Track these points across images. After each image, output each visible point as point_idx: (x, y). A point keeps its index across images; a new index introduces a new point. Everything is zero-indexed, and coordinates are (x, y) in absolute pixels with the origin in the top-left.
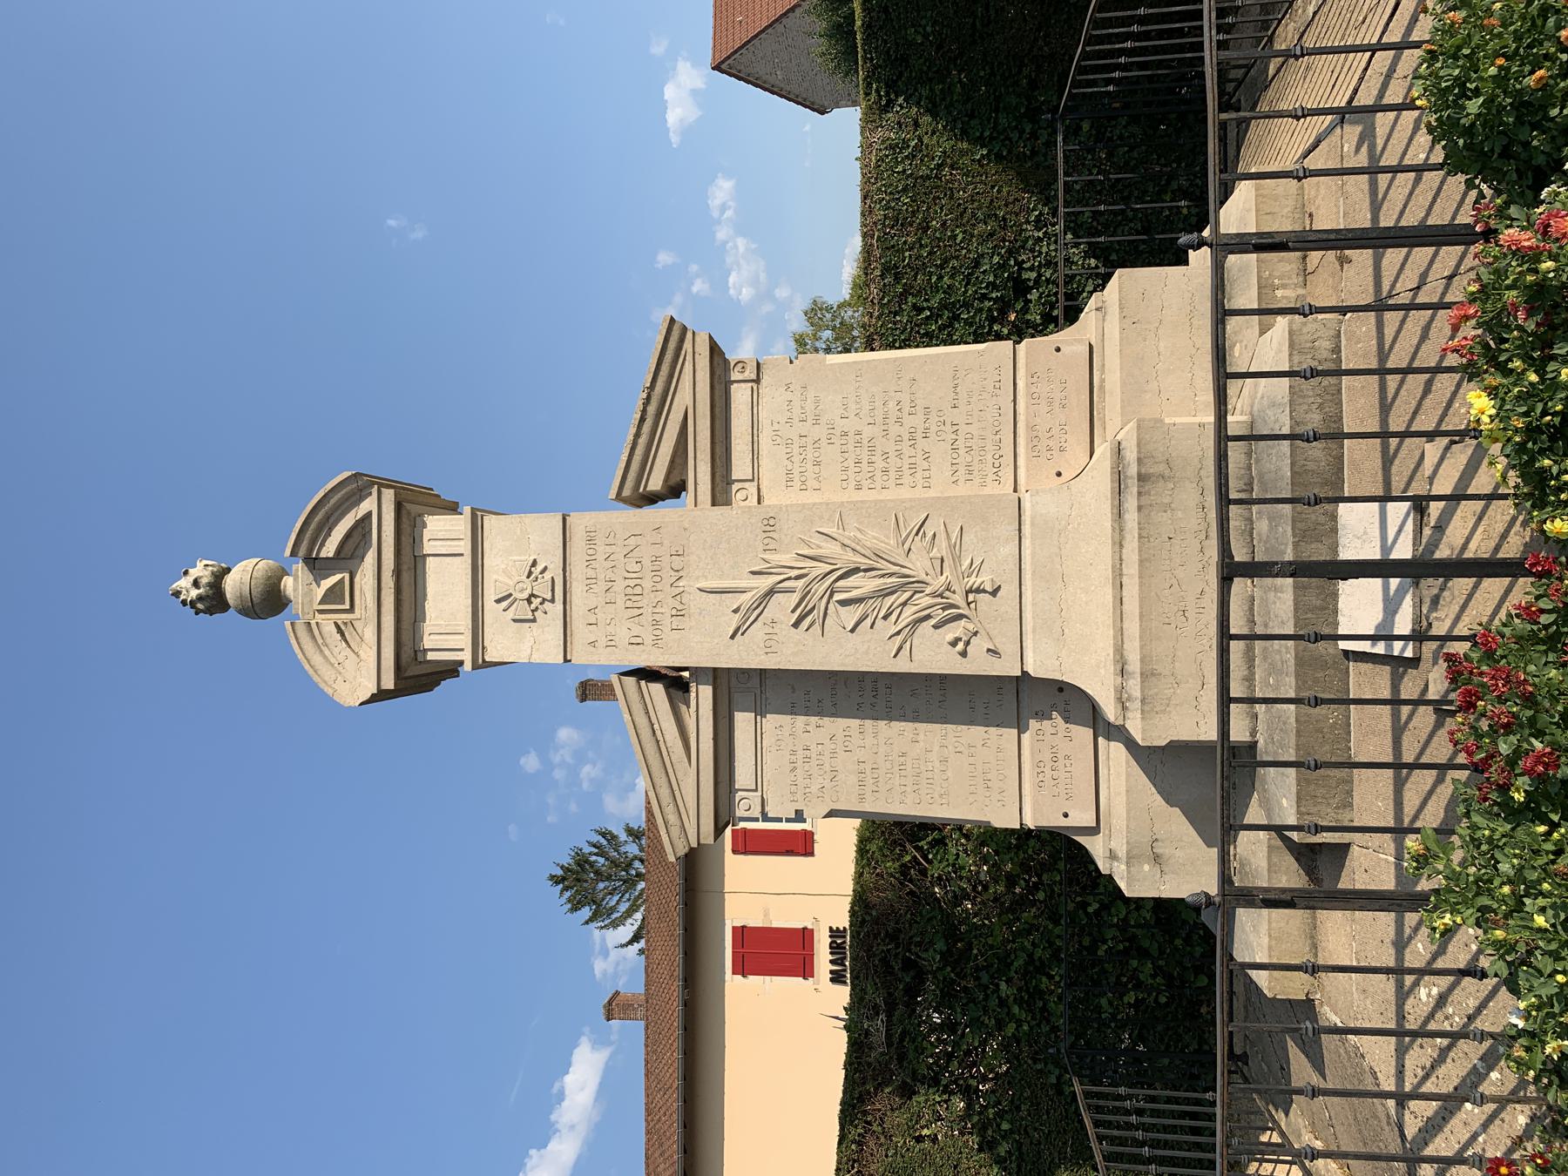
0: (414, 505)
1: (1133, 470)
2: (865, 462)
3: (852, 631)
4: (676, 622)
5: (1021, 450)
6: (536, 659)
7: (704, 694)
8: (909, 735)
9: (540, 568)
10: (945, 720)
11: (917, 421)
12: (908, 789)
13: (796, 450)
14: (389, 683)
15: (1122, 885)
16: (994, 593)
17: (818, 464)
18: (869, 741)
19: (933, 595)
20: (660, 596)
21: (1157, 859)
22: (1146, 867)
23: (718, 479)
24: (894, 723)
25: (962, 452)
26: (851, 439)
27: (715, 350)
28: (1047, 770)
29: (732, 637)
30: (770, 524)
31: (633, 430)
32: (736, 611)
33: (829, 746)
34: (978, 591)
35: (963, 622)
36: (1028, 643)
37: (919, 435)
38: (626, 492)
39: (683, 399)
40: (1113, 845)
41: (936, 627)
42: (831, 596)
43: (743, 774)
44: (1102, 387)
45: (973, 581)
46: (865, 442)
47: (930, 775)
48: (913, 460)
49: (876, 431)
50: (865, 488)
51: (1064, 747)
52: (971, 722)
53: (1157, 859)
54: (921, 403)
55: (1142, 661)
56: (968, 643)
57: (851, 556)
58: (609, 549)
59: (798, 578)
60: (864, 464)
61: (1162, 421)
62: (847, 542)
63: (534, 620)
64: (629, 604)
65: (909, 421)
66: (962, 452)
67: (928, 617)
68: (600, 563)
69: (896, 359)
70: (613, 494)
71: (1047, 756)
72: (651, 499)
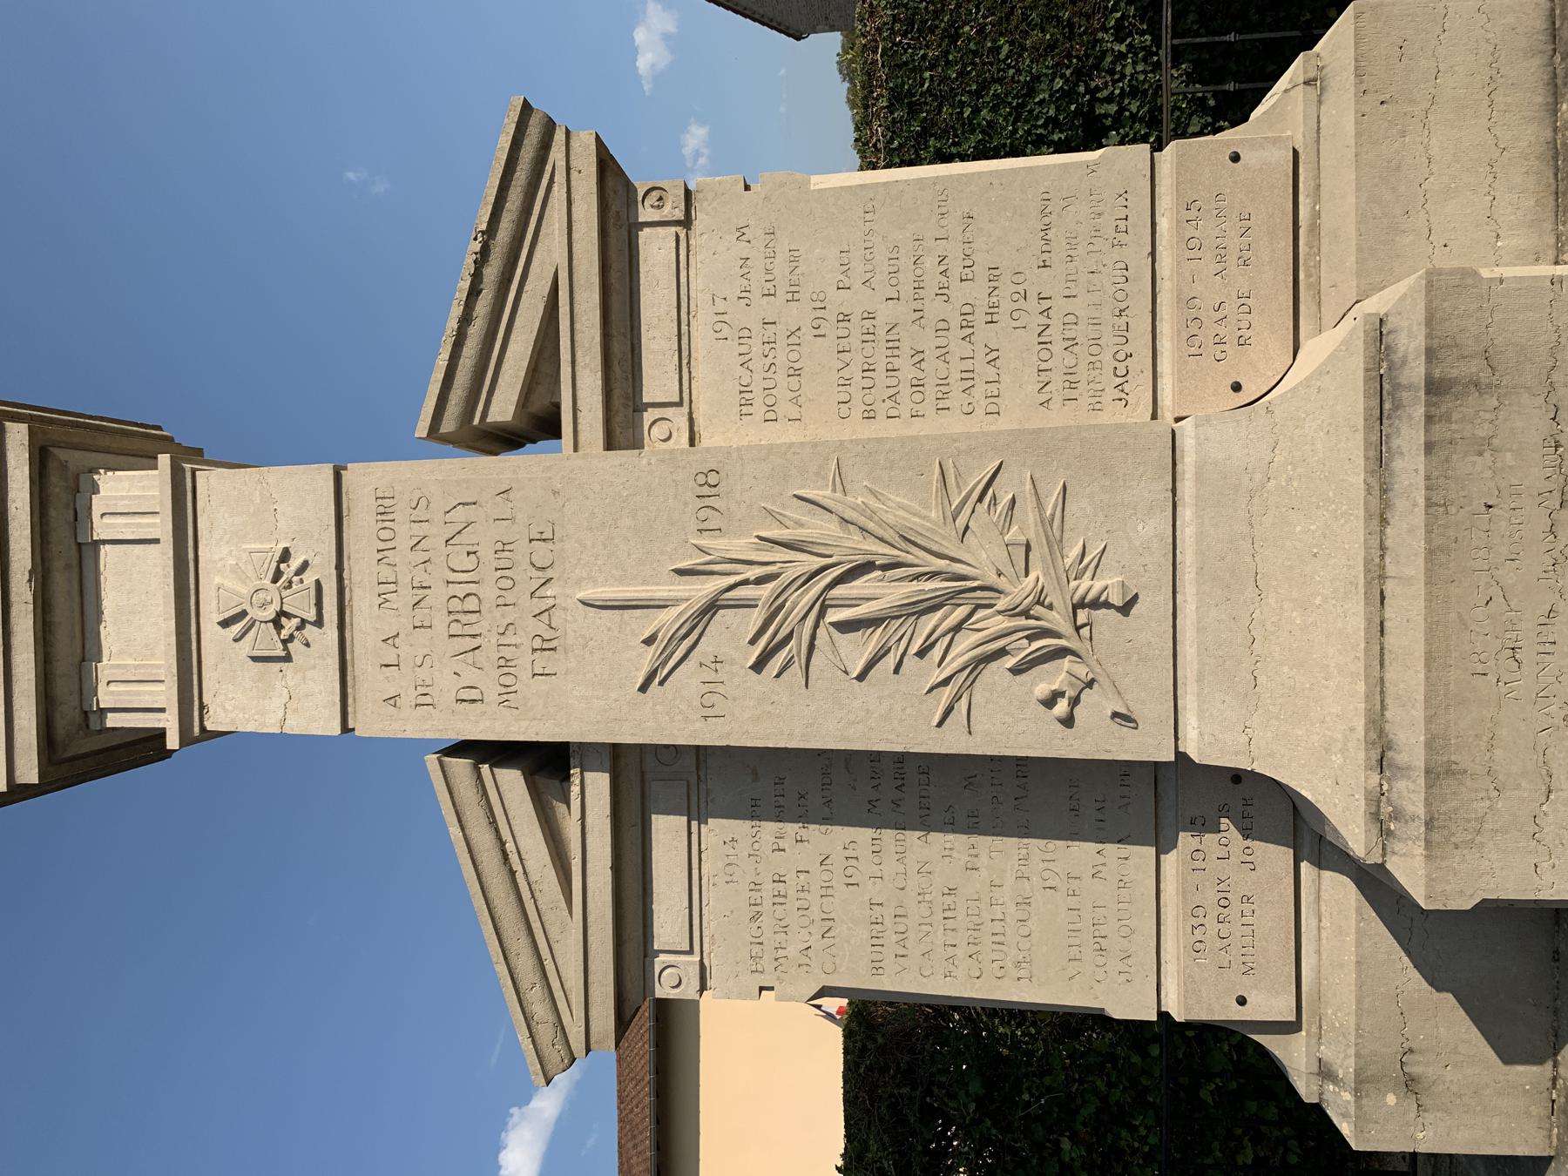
0: (70, 452)
1: (1415, 372)
3: (861, 677)
4: (541, 660)
5: (1165, 345)
6: (295, 726)
7: (594, 790)
8: (961, 857)
9: (295, 563)
10: (1024, 830)
11: (977, 293)
12: (961, 952)
13: (757, 349)
14: (29, 773)
15: (1345, 1129)
16: (1125, 609)
17: (796, 373)
18: (890, 866)
19: (1011, 612)
20: (511, 614)
21: (1411, 1085)
22: (1391, 1099)
23: (617, 401)
24: (935, 837)
25: (1058, 347)
27: (606, 165)
28: (1212, 926)
29: (643, 688)
30: (709, 484)
31: (457, 311)
32: (649, 641)
33: (818, 876)
34: (1096, 604)
35: (1067, 662)
36: (1188, 701)
37: (980, 318)
38: (448, 425)
39: (548, 254)
40: (1325, 1052)
41: (1016, 671)
42: (822, 614)
43: (668, 926)
44: (1314, 228)
45: (1088, 586)
47: (998, 927)
48: (967, 365)
49: (902, 311)
50: (881, 416)
51: (1242, 881)
52: (1073, 834)
53: (1411, 1085)
54: (982, 260)
55: (1429, 745)
56: (1075, 702)
57: (856, 540)
58: (419, 530)
59: (760, 581)
61: (1475, 273)
62: (849, 514)
63: (287, 658)
64: (456, 629)
66: (1058, 347)
67: (1002, 652)
68: (402, 555)
70: (422, 429)
71: (1210, 896)
72: (504, 440)
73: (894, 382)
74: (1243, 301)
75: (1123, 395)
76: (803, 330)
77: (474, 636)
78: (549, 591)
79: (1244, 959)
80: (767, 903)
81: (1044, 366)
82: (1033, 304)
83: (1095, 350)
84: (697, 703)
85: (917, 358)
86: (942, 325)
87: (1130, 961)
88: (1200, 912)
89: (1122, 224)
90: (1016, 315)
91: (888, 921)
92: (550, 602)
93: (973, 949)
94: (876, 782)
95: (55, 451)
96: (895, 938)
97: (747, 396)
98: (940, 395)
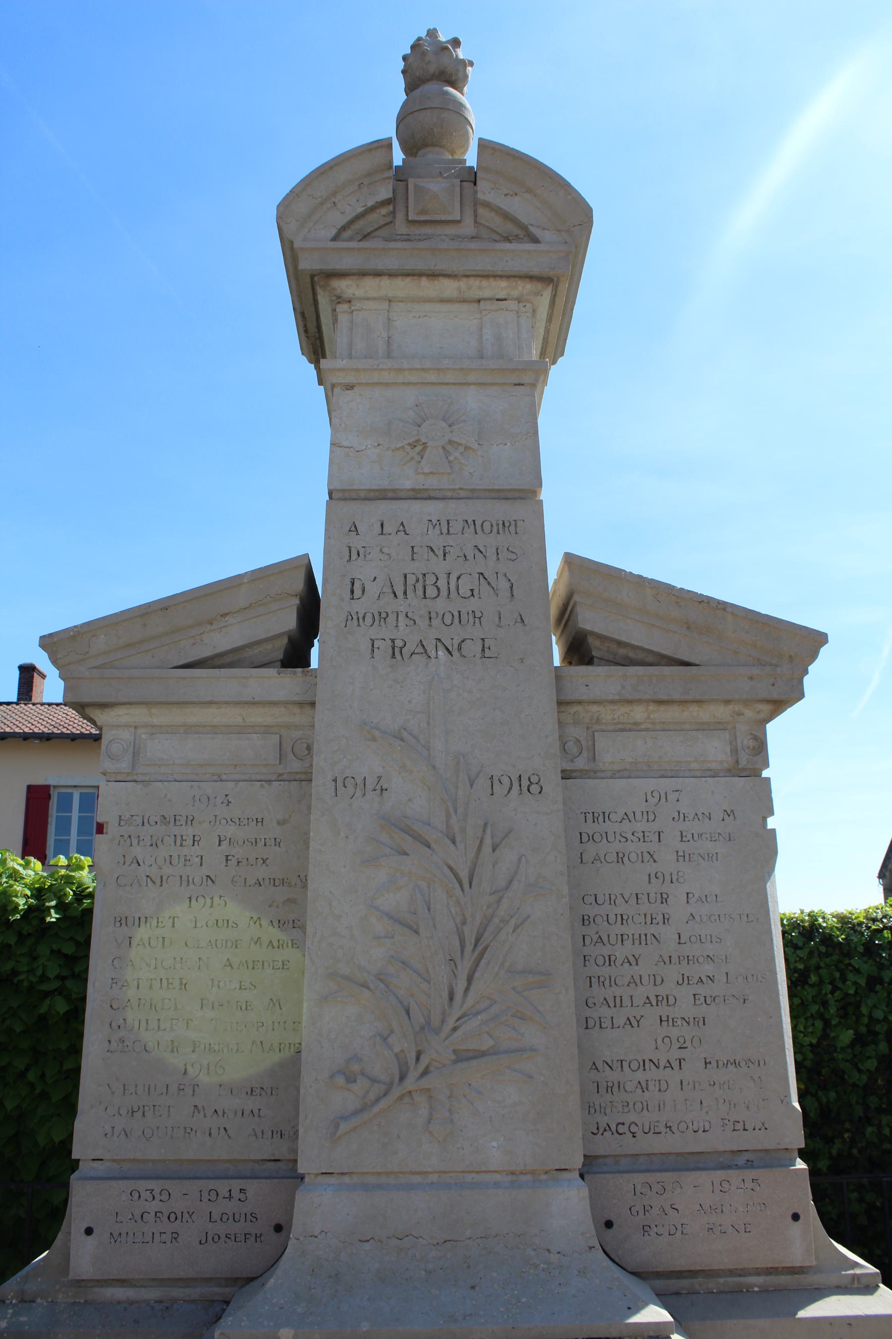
2: (624, 929)
4: (384, 647)
11: (685, 1008)
13: (640, 826)
20: (422, 623)
25: (640, 1075)
37: (664, 1011)
46: (653, 929)
48: (627, 1002)
58: (491, 552)
60: (618, 929)
64: (411, 580)
66: (640, 1075)
69: (774, 973)
73: (613, 941)
74: (679, 1228)
75: (601, 1132)
76: (654, 865)
77: (405, 593)
78: (441, 653)
81: (625, 1064)
82: (676, 1054)
83: (638, 1106)
85: (632, 959)
87: (123, 1136)
88: (165, 1196)
89: (739, 1126)
90: (667, 1040)
92: (433, 654)
95: (547, 293)
97: (601, 818)
98: (602, 979)
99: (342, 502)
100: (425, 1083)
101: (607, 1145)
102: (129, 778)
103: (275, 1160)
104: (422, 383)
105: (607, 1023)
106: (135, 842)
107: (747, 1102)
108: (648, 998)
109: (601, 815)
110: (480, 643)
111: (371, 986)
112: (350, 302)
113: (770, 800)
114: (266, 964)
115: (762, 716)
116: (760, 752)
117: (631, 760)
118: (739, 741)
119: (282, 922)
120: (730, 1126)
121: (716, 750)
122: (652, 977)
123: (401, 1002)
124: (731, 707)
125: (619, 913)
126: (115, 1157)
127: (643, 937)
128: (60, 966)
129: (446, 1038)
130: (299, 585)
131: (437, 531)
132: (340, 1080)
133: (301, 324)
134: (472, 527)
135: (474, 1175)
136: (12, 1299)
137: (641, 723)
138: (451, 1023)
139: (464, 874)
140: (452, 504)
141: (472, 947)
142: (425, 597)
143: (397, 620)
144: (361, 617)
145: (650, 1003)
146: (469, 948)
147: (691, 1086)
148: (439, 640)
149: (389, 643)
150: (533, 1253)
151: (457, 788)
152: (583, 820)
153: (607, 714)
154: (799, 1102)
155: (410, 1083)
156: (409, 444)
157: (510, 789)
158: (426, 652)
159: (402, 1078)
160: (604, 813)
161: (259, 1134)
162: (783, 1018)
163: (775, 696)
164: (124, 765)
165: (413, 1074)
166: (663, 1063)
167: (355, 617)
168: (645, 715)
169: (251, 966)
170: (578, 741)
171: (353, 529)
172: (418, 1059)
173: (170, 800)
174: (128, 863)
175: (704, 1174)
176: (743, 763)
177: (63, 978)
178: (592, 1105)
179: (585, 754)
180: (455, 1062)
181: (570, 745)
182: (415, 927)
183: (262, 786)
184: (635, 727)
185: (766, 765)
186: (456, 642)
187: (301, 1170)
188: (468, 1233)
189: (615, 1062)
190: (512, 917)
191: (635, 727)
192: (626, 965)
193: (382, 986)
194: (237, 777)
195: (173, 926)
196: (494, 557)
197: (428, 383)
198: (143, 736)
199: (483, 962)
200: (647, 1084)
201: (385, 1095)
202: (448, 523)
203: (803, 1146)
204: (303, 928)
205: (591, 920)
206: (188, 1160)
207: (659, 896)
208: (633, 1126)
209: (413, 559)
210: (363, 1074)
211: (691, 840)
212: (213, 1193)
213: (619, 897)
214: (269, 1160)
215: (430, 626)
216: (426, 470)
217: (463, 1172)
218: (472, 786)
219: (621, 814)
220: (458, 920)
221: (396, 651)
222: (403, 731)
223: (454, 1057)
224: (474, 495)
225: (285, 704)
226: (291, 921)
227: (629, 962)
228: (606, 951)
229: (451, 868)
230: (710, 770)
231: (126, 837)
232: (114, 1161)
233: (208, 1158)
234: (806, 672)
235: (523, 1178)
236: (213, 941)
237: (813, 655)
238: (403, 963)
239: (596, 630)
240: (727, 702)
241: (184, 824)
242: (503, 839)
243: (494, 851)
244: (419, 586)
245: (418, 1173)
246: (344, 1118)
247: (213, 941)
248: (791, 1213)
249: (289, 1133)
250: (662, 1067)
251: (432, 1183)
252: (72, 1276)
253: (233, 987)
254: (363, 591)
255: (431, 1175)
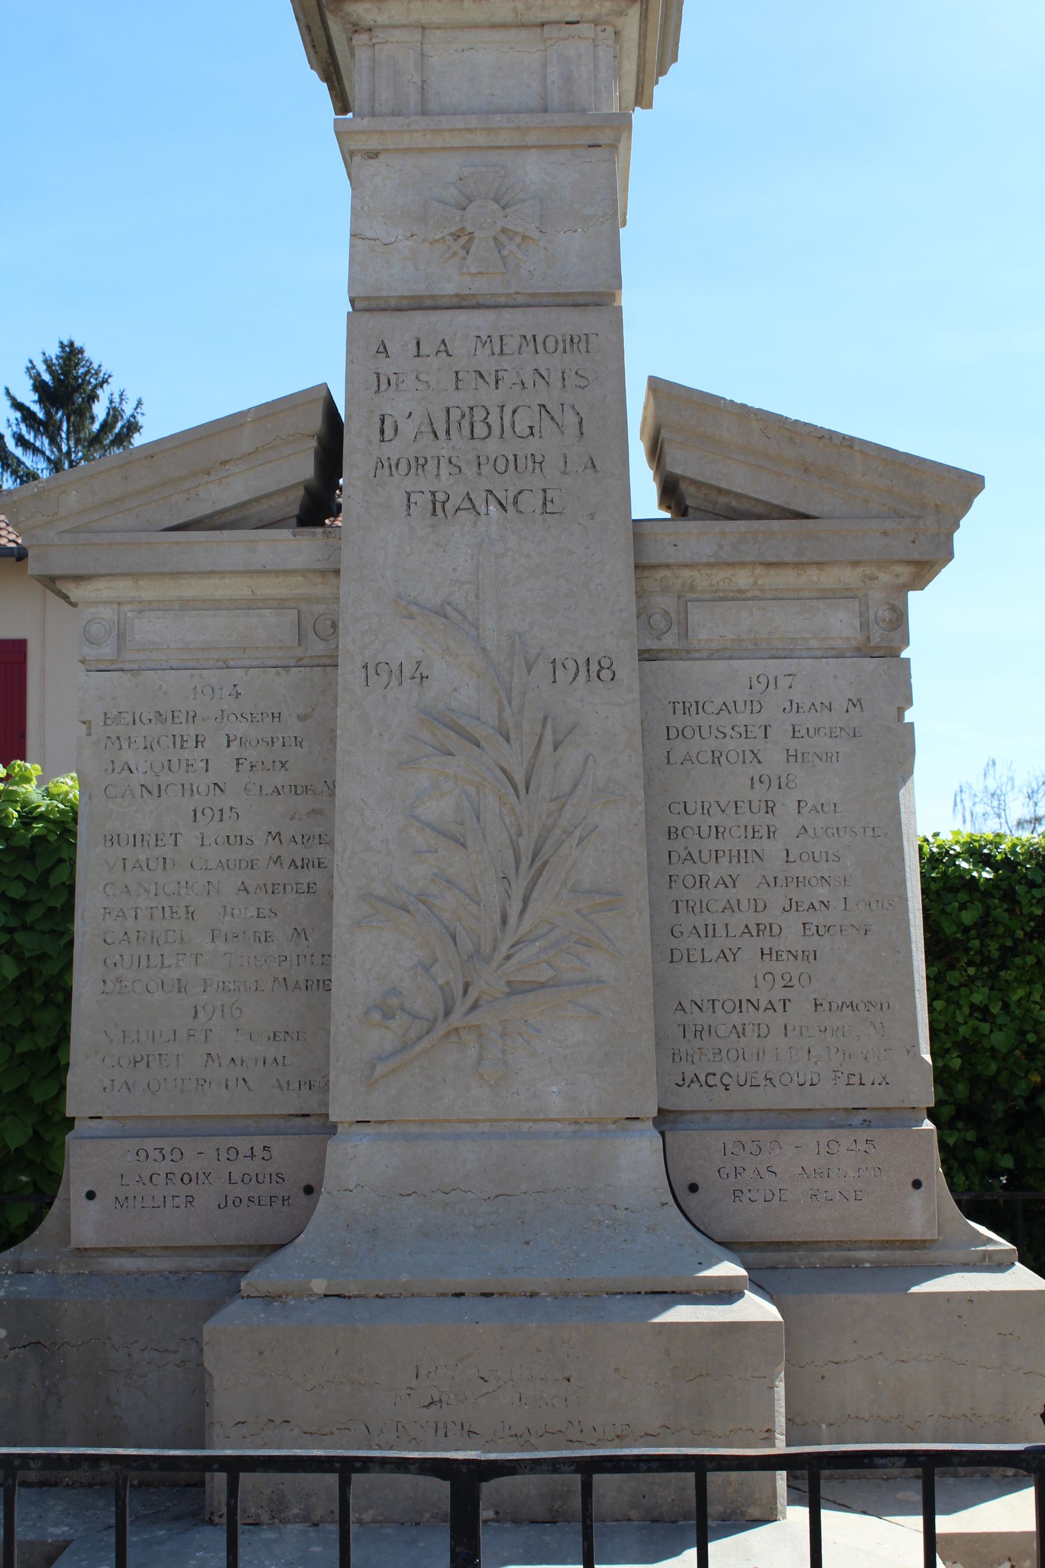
2: (719, 844)
11: (792, 938)
12: (130, 922)
13: (743, 718)
20: (470, 471)
25: (735, 1018)
26: (762, 820)
28: (163, 1167)
37: (766, 942)
46: (755, 845)
47: (155, 960)
48: (721, 931)
58: (555, 378)
60: (712, 844)
64: (455, 414)
65: (792, 923)
69: (904, 899)
73: (705, 858)
74: (777, 1193)
76: (759, 766)
77: (448, 432)
79: (131, 1199)
80: (175, 730)
83: (733, 1054)
84: (381, 658)
85: (728, 880)
86: (760, 906)
87: (124, 1090)
88: (177, 1155)
89: (855, 1080)
90: (769, 977)
91: (159, 852)
92: (482, 509)
93: (133, 936)
94: (299, 839)
96: (143, 858)
97: (693, 709)
98: (691, 904)
99: (367, 315)
100: (474, 1019)
101: (692, 1099)
102: (114, 667)
103: (304, 1115)
104: (467, 148)
105: (696, 956)
106: (125, 745)
107: (865, 1052)
108: (746, 926)
109: (694, 705)
110: (541, 495)
111: (411, 908)
112: (370, 30)
113: (909, 686)
114: (288, 887)
115: (902, 580)
116: (899, 626)
117: (732, 636)
118: (871, 613)
119: (306, 838)
120: (844, 1079)
121: (841, 624)
122: (752, 902)
123: (446, 927)
124: (860, 570)
125: (714, 824)
126: (117, 1114)
127: (743, 854)
128: (5, 913)
129: (499, 967)
130: (316, 422)
131: (488, 351)
132: (376, 1016)
133: (308, 38)
134: (532, 344)
135: (531, 1124)
136: (7, 1269)
137: (748, 591)
138: (504, 949)
139: (519, 778)
140: (507, 314)
141: (529, 863)
142: (473, 438)
143: (438, 468)
144: (393, 463)
145: (750, 932)
146: (525, 863)
147: (797, 1032)
148: (490, 492)
149: (429, 496)
150: (597, 1209)
151: (511, 674)
152: (672, 711)
153: (703, 580)
154: (932, 1054)
155: (456, 1019)
156: (451, 234)
157: (576, 675)
158: (474, 507)
159: (447, 1013)
160: (697, 703)
161: (285, 1086)
162: (914, 954)
163: (916, 557)
164: (107, 651)
165: (460, 1009)
166: (763, 1005)
167: (386, 464)
168: (752, 580)
169: (270, 890)
170: (667, 613)
171: (382, 349)
172: (465, 992)
173: (165, 693)
174: (118, 770)
175: (808, 1132)
176: (875, 640)
177: (11, 931)
178: (677, 1052)
179: (675, 629)
180: (509, 995)
181: (657, 619)
182: (462, 840)
183: (278, 673)
184: (739, 596)
185: (906, 642)
186: (511, 495)
187: (333, 1118)
188: (524, 1187)
189: (705, 1002)
190: (576, 827)
191: (739, 596)
192: (721, 887)
193: (423, 908)
194: (247, 663)
195: (176, 845)
196: (559, 384)
197: (476, 147)
198: (129, 614)
199: (541, 880)
200: (744, 1029)
201: (427, 1033)
202: (502, 340)
203: (933, 1105)
204: (331, 844)
205: (679, 832)
206: (202, 1116)
207: (763, 804)
208: (726, 1077)
209: (457, 388)
210: (402, 1009)
211: (806, 736)
212: (233, 1152)
213: (714, 805)
214: (297, 1116)
215: (479, 474)
216: (473, 270)
217: (519, 1120)
218: (529, 672)
219: (718, 701)
220: (513, 831)
221: (437, 506)
222: (447, 607)
223: (507, 990)
224: (533, 302)
225: (303, 572)
226: (317, 837)
227: (724, 883)
228: (697, 870)
229: (504, 771)
230: (834, 649)
231: (114, 738)
232: (115, 1118)
233: (225, 1113)
234: (957, 525)
235: (587, 1127)
236: (224, 861)
237: (966, 504)
238: (449, 882)
239: (689, 474)
240: (855, 564)
241: (184, 720)
242: (566, 736)
243: (555, 749)
244: (466, 423)
245: (466, 1121)
246: (381, 1059)
247: (224, 861)
248: (911, 1179)
249: (317, 1083)
250: (762, 1009)
251: (483, 1133)
252: (74, 1244)
253: (250, 915)
254: (396, 430)
255: (481, 1124)
